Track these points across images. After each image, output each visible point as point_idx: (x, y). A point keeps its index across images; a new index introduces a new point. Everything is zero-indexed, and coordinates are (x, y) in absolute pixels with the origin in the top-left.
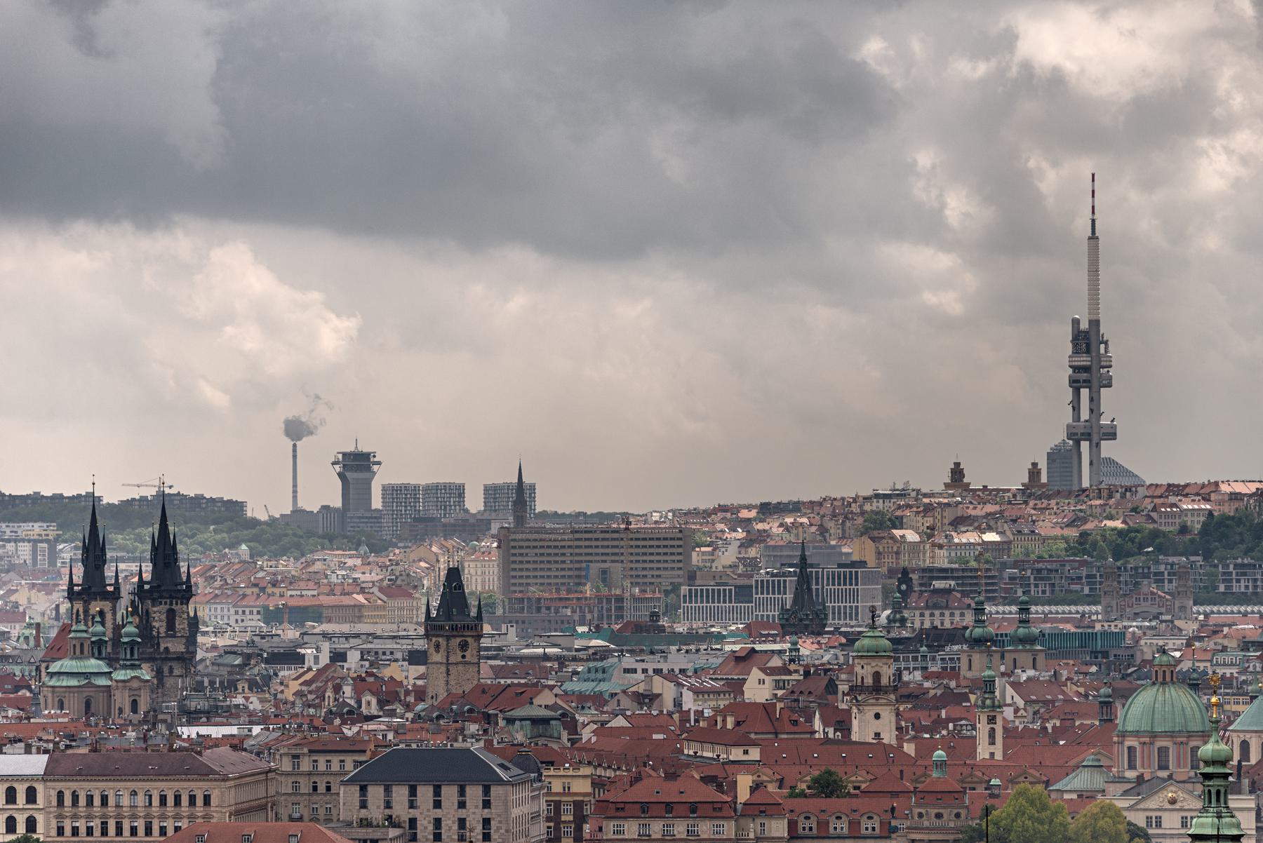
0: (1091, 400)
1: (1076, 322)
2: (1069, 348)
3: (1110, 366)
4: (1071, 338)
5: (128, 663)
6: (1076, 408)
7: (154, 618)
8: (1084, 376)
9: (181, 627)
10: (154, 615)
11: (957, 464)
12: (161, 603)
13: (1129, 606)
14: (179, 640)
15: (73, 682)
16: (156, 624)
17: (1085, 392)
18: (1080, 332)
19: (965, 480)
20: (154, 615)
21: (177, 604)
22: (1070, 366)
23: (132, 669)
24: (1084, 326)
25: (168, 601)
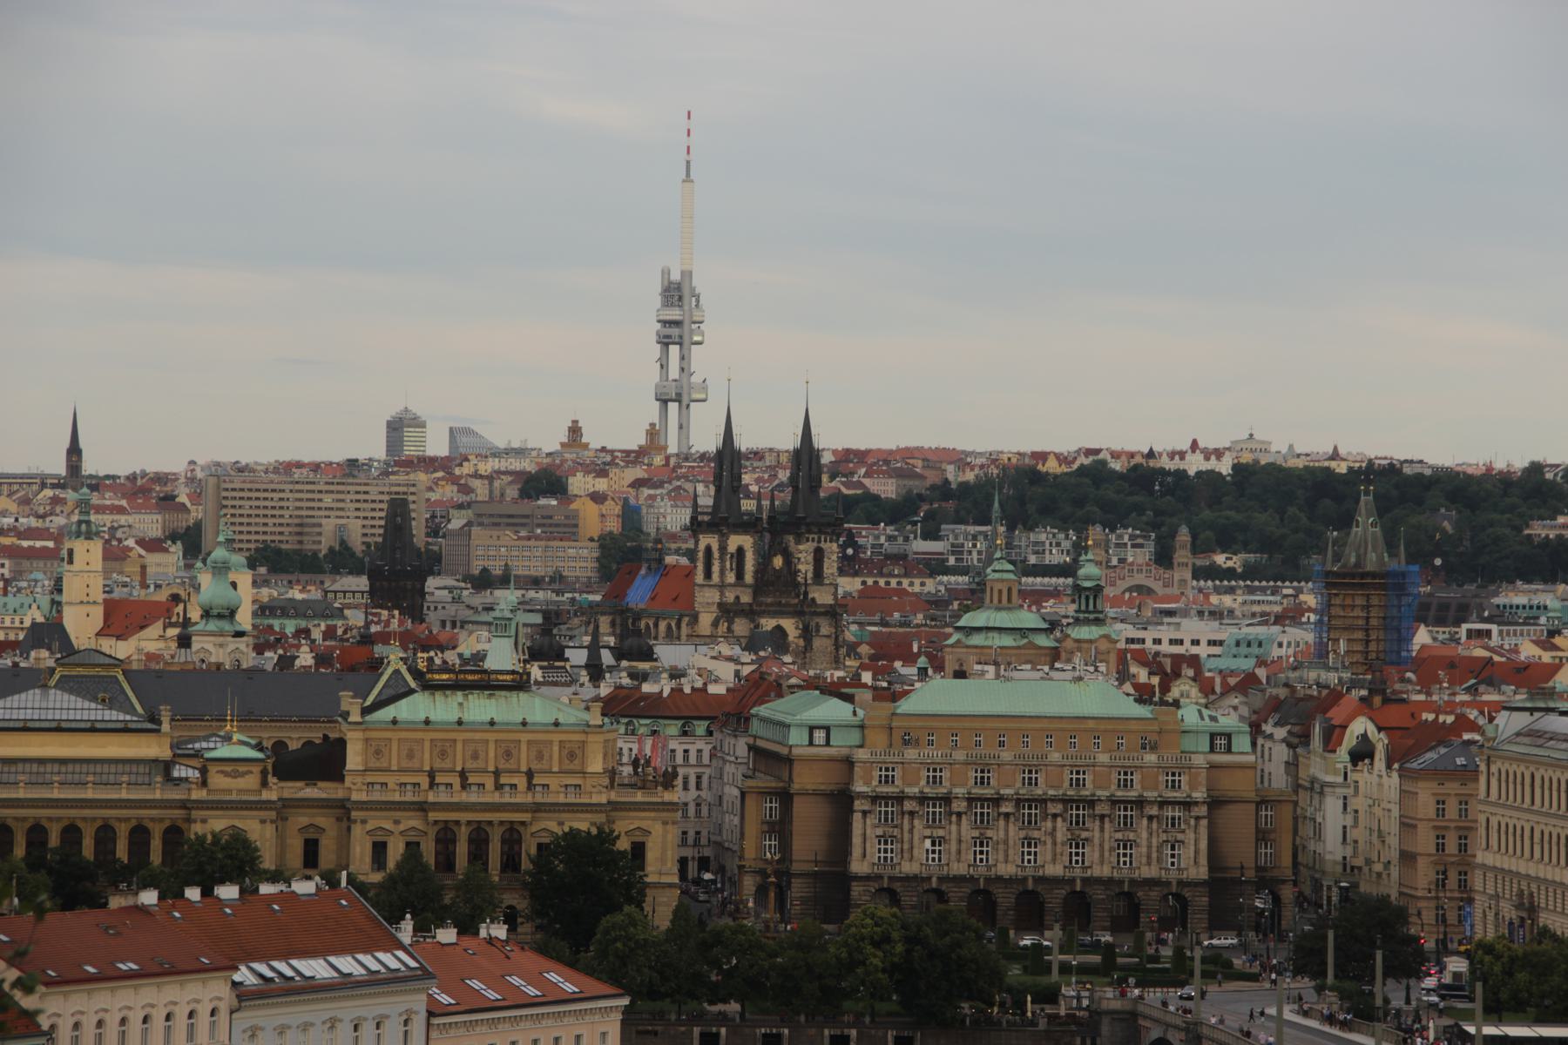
0: (682, 358)
1: (666, 272)
2: (657, 301)
3: (701, 322)
4: (660, 290)
5: (1092, 616)
6: (664, 366)
7: (799, 559)
8: (675, 331)
9: (830, 571)
10: (800, 555)
11: (575, 422)
12: (808, 540)
13: (1120, 579)
14: (827, 588)
15: (1007, 641)
16: (802, 567)
17: (674, 350)
18: (670, 283)
19: (584, 440)
20: (800, 555)
21: (825, 541)
22: (659, 321)
23: (1097, 625)
24: (676, 276)
25: (816, 537)
